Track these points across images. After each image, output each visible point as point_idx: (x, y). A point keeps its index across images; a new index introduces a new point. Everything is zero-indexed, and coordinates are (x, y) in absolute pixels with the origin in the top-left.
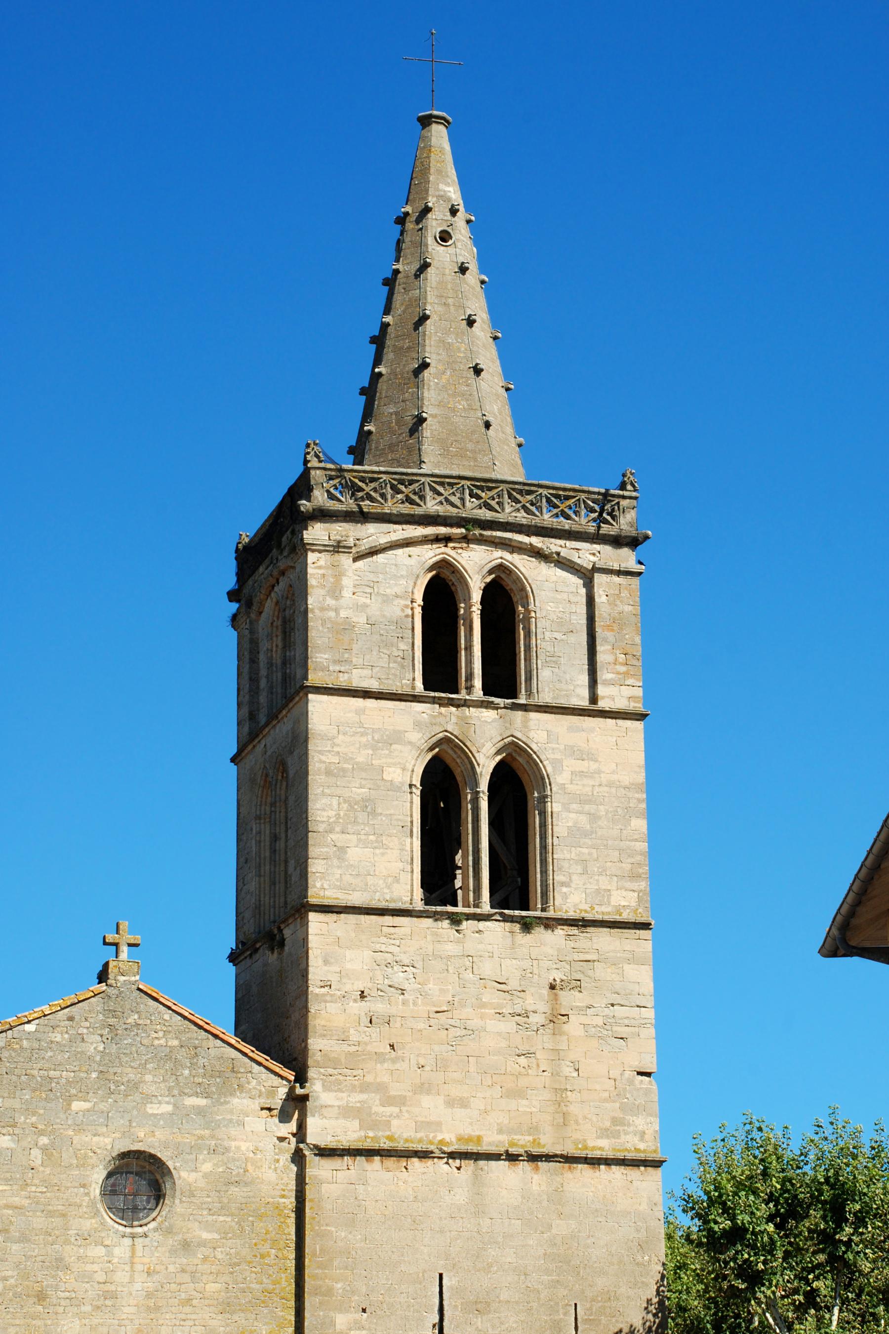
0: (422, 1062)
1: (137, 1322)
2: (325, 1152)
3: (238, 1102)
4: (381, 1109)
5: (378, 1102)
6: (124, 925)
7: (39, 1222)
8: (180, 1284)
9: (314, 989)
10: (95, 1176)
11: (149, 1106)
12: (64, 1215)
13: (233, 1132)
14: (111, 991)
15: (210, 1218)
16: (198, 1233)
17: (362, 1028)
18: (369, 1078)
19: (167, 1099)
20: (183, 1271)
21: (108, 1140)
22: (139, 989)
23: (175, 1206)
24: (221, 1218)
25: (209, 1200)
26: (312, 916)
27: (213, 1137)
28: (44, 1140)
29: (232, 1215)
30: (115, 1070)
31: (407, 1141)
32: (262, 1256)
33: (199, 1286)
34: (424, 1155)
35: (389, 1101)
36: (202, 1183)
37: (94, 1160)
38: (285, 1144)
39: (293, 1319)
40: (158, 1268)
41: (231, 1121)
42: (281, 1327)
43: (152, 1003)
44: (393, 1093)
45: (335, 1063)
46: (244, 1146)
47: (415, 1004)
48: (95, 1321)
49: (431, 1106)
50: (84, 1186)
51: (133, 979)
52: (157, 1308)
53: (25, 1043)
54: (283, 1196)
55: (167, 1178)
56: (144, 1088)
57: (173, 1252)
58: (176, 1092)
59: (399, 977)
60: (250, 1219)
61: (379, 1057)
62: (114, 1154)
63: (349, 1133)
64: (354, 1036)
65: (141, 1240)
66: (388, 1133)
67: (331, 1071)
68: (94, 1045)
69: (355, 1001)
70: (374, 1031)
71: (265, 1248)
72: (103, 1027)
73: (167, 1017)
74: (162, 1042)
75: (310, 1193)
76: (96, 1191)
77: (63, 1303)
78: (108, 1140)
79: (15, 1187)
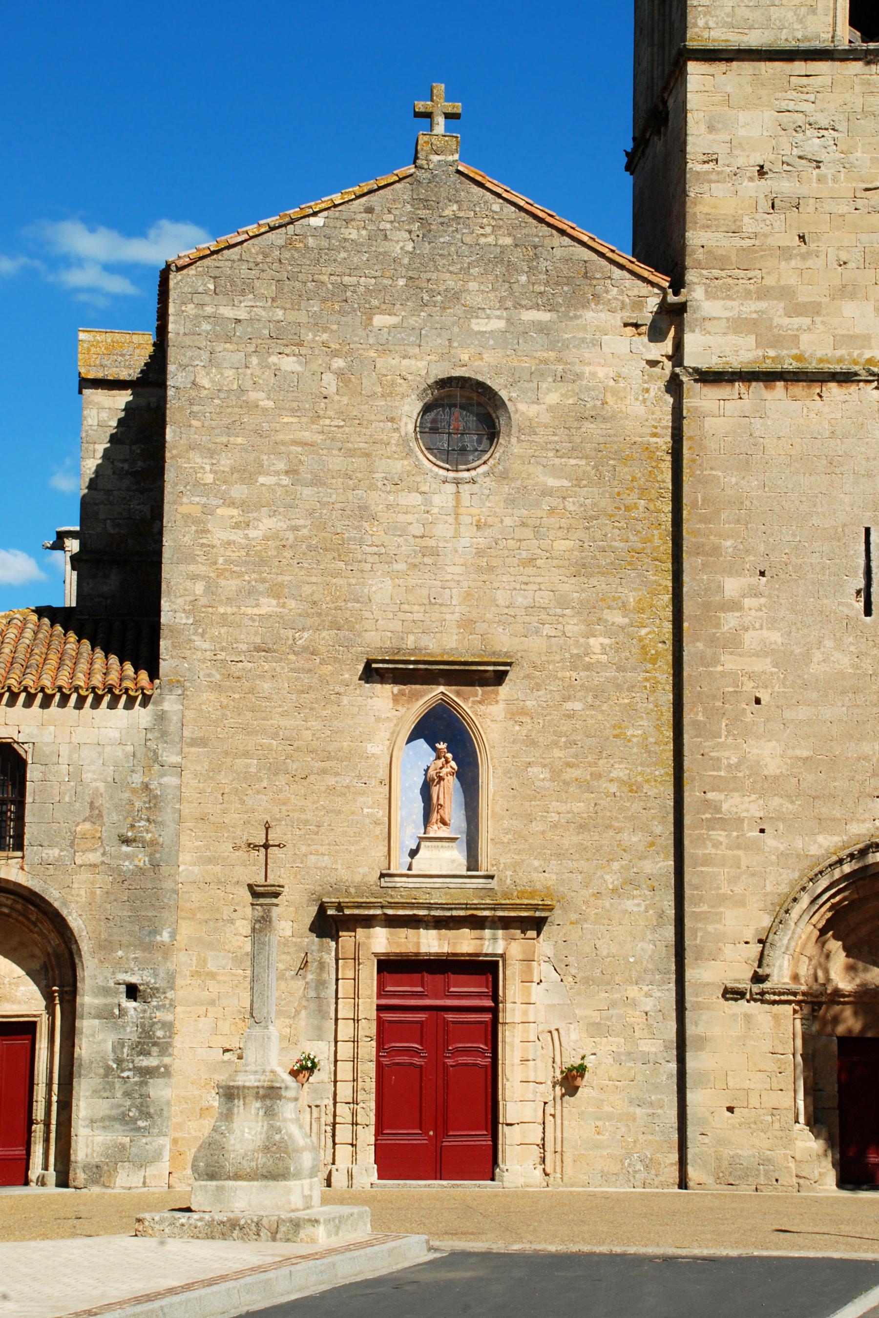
0: (844, 257)
1: (465, 584)
2: (709, 377)
3: (593, 316)
4: (786, 321)
5: (781, 312)
6: (440, 88)
7: (336, 462)
8: (520, 540)
9: (694, 166)
10: (406, 408)
11: (473, 321)
12: (367, 455)
13: (587, 354)
14: (422, 175)
15: (557, 461)
16: (542, 478)
17: (760, 216)
18: (770, 281)
19: (498, 313)
20: (524, 525)
21: (421, 364)
22: (458, 172)
23: (511, 447)
24: (573, 462)
25: (556, 438)
26: (692, 67)
27: (559, 360)
28: (339, 363)
29: (587, 457)
30: (429, 275)
31: (821, 360)
32: (628, 509)
33: (545, 544)
34: (845, 378)
35: (797, 309)
36: (546, 418)
37: (403, 388)
38: (657, 370)
39: (670, 584)
40: (490, 520)
41: (583, 340)
42: (654, 593)
43: (475, 189)
44: (801, 299)
45: (722, 262)
46: (601, 372)
47: (835, 180)
48: (411, 582)
49: (855, 315)
50: (392, 420)
51: (450, 158)
52: (491, 569)
53: (311, 241)
54: (655, 435)
55: (500, 412)
56: (468, 299)
57: (510, 502)
58: (509, 304)
59: (813, 145)
60: (611, 462)
61: (785, 253)
62: (431, 381)
63: (742, 353)
64: (749, 225)
65: (467, 486)
66: (795, 351)
67: (716, 273)
68: (400, 244)
69: (751, 179)
70: (777, 219)
71: (632, 498)
72: (411, 221)
73: (496, 208)
74: (491, 240)
75: (688, 429)
76: (408, 426)
77: (370, 559)
78: (421, 364)
79: (304, 420)
